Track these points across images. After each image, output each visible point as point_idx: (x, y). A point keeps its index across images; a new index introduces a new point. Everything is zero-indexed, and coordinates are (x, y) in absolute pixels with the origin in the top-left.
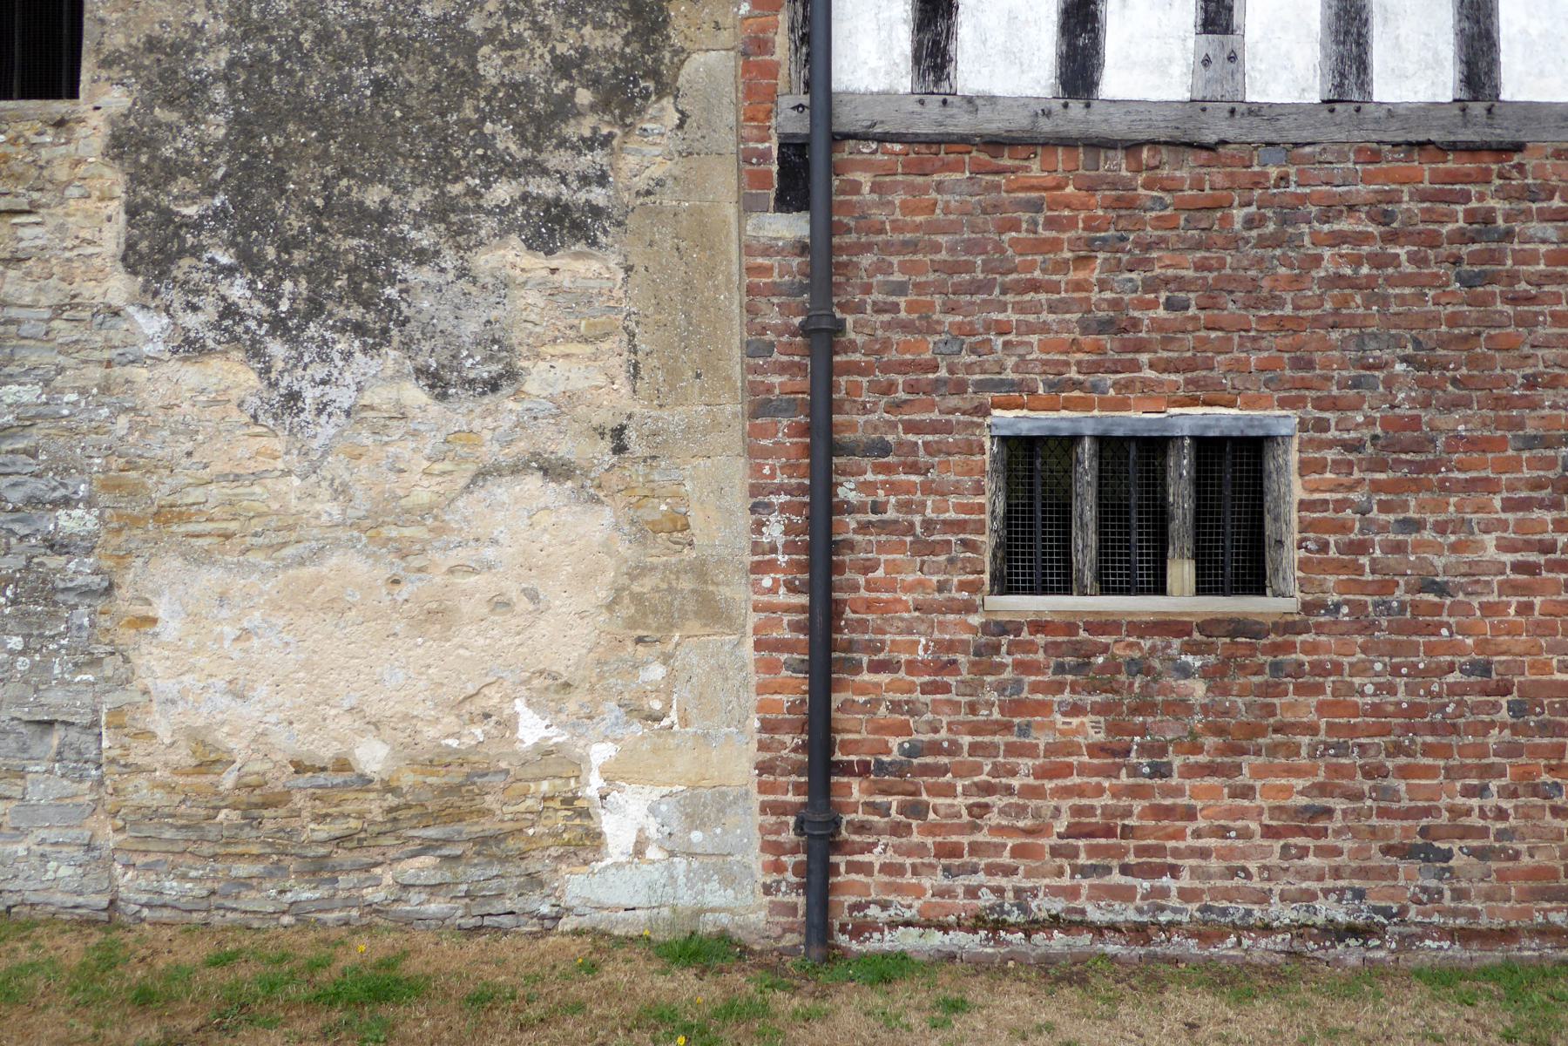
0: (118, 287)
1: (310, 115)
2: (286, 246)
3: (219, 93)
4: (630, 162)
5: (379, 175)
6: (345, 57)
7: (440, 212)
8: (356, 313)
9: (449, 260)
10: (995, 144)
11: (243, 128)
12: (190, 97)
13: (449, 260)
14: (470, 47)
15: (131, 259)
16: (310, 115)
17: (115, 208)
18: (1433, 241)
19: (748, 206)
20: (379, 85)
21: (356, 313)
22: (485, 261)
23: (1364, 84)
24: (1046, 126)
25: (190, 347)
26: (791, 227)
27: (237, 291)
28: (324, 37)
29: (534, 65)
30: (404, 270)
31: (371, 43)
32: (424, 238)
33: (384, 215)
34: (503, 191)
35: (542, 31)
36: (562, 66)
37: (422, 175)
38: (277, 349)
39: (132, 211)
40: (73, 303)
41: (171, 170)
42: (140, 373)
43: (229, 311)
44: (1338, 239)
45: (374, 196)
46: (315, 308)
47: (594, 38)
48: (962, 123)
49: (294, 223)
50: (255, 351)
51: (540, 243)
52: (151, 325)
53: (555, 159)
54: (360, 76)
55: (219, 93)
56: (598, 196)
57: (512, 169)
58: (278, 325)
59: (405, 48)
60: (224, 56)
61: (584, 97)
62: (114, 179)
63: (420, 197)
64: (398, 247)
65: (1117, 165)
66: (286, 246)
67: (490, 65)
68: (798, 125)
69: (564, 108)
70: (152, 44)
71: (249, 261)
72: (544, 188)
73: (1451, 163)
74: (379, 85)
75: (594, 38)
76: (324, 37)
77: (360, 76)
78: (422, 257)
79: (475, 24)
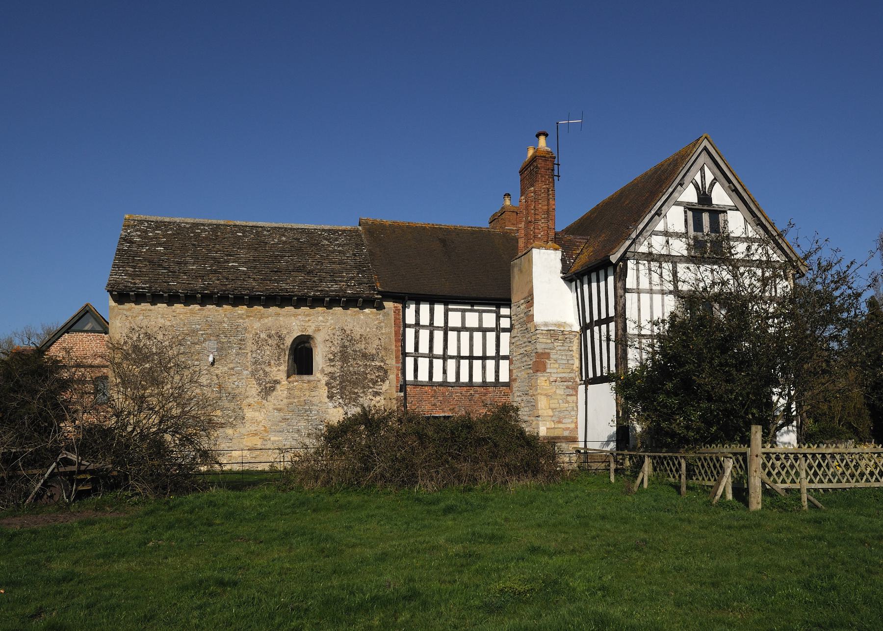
0: (327, 400)
1: (349, 381)
2: (346, 396)
3: (338, 378)
4: (384, 387)
5: (357, 388)
6: (352, 375)
7: (364, 392)
8: (354, 403)
9: (365, 398)
10: (422, 386)
12: (335, 379)
13: (365, 398)
14: (367, 374)
15: (328, 397)
16: (349, 381)
17: (326, 391)
18: (466, 396)
19: (397, 392)
20: (356, 378)
21: (354, 403)
24: (428, 384)
25: (335, 407)
26: (402, 394)
27: (341, 401)
28: (350, 373)
29: (373, 377)
30: (360, 399)
31: (355, 373)
32: (362, 395)
33: (357, 393)
34: (370, 390)
35: (375, 373)
36: (377, 377)
37: (361, 388)
39: (328, 392)
40: (321, 402)
42: (329, 410)
43: (340, 403)
44: (457, 396)
45: (356, 391)
47: (380, 374)
48: (419, 383)
49: (347, 394)
50: (343, 408)
52: (331, 404)
53: (376, 387)
54: (354, 377)
55: (338, 378)
56: (381, 391)
57: (371, 388)
58: (345, 405)
59: (359, 374)
60: (338, 374)
61: (379, 380)
62: (326, 388)
63: (361, 391)
64: (359, 396)
65: (435, 388)
66: (346, 396)
67: (369, 376)
69: (377, 381)
70: (330, 373)
71: (342, 398)
72: (375, 390)
73: (468, 388)
74: (356, 378)
75: (380, 374)
76: (350, 373)
77: (354, 377)
78: (362, 397)
79: (367, 372)
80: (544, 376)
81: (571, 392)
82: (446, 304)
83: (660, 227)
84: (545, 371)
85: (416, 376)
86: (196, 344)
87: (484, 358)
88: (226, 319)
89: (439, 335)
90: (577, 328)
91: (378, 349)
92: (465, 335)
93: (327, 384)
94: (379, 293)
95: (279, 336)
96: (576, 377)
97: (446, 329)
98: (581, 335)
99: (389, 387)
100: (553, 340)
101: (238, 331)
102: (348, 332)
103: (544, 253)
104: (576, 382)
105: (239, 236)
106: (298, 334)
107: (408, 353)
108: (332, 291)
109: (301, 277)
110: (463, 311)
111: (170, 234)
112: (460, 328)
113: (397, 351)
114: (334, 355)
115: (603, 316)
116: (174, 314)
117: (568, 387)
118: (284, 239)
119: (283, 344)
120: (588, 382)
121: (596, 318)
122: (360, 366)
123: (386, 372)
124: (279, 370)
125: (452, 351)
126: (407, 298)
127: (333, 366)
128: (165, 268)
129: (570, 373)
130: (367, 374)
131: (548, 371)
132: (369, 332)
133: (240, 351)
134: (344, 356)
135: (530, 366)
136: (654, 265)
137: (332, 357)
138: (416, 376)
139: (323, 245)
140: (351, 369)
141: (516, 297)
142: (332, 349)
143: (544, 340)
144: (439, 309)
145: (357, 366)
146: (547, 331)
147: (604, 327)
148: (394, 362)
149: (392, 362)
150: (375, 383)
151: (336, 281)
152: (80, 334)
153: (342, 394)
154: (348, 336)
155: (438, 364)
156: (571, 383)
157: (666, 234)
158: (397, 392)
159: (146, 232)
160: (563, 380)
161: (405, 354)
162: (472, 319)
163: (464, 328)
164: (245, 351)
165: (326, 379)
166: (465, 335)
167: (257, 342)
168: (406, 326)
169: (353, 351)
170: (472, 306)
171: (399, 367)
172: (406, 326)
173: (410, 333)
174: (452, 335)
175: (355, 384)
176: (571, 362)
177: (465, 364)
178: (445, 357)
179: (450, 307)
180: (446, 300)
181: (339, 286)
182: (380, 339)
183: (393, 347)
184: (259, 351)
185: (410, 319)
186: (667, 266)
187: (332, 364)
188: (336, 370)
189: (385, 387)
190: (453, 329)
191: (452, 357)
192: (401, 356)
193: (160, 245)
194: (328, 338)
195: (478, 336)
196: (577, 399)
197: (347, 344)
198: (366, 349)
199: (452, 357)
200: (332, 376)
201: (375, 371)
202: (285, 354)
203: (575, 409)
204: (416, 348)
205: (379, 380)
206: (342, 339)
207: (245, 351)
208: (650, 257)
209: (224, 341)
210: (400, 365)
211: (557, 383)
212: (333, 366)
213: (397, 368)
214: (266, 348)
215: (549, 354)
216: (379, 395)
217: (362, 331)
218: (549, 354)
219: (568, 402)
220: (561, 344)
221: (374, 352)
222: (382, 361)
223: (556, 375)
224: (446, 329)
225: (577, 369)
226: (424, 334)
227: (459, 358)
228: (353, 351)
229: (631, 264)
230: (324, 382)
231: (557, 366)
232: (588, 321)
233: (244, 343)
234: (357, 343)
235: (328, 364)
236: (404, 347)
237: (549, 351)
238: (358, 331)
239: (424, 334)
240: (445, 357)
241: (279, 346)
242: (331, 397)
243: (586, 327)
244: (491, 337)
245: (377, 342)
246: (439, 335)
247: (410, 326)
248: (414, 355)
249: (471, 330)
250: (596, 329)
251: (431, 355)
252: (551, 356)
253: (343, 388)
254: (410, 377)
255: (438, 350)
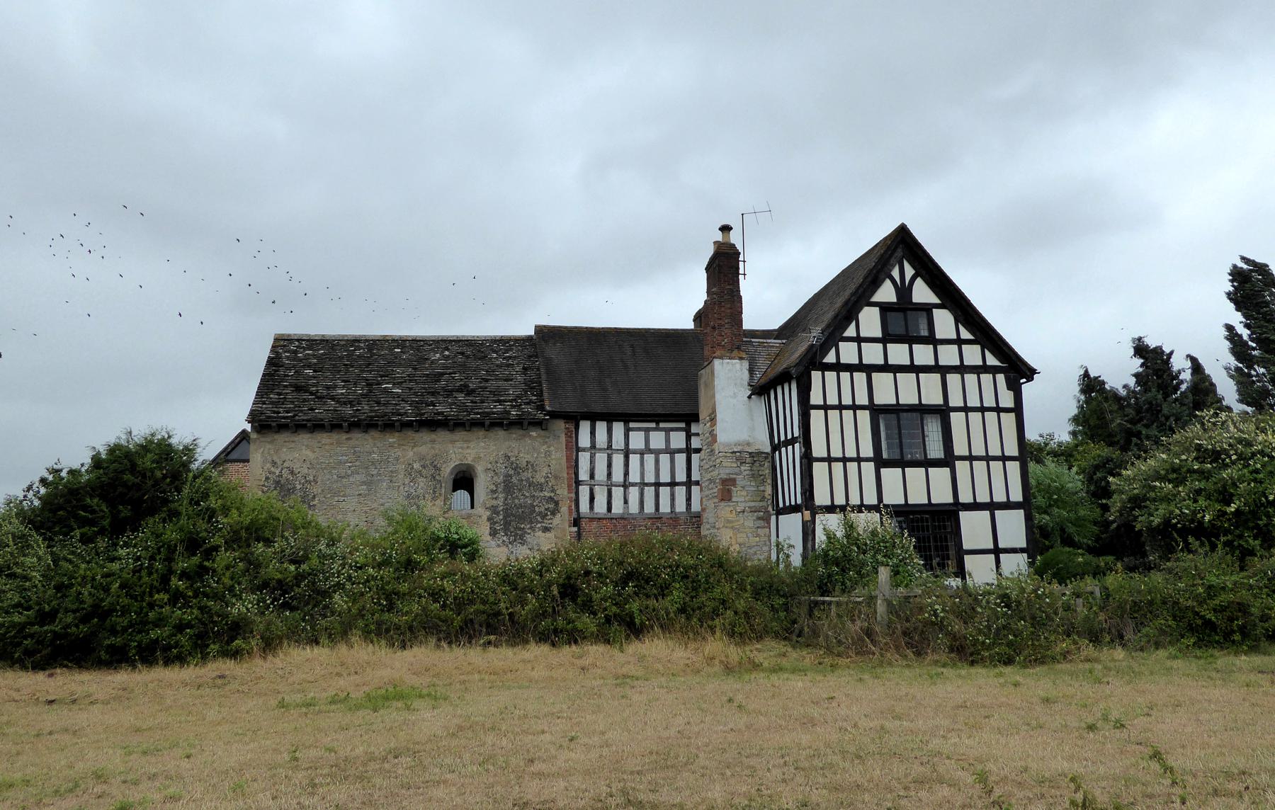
0: (489, 538)
3: (501, 513)
7: (531, 528)
10: (599, 519)
11: (505, 517)
14: (534, 507)
15: (490, 535)
17: (488, 528)
19: (570, 526)
22: (536, 534)
23: (644, 511)
24: (606, 517)
25: (499, 546)
26: (575, 529)
27: (505, 538)
29: (543, 510)
32: (529, 531)
33: (524, 528)
34: (539, 525)
35: (543, 505)
36: (546, 509)
37: (528, 524)
38: (510, 546)
41: (496, 523)
43: (504, 541)
45: (522, 526)
46: (515, 540)
47: (550, 506)
48: (595, 516)
49: (512, 530)
50: (507, 546)
51: (544, 532)
53: (545, 521)
55: (501, 513)
56: (551, 526)
57: (541, 523)
58: (510, 543)
60: (502, 508)
63: (528, 526)
64: (526, 532)
67: (537, 509)
68: (576, 516)
69: (547, 515)
70: (492, 506)
71: (506, 535)
75: (550, 506)
76: (515, 505)
78: (529, 534)
79: (535, 504)
80: (729, 506)
81: (761, 523)
82: (626, 422)
83: (851, 331)
84: (730, 500)
85: (592, 508)
86: (343, 477)
87: (673, 484)
88: (375, 449)
89: (618, 460)
90: (768, 449)
91: (548, 477)
92: (650, 459)
93: (489, 519)
94: (549, 413)
95: (435, 466)
96: (768, 506)
97: (627, 453)
98: (773, 458)
99: (561, 521)
100: (739, 463)
101: (389, 462)
102: (513, 459)
103: (728, 363)
104: (769, 511)
105: (398, 352)
106: (456, 463)
107: (581, 481)
108: (494, 413)
109: (461, 397)
110: (647, 430)
111: (322, 354)
112: (642, 450)
113: (569, 479)
114: (496, 486)
115: (789, 437)
116: (320, 445)
117: (759, 518)
118: (447, 353)
119: (439, 474)
120: (780, 512)
121: (783, 438)
122: (527, 497)
123: (557, 503)
124: (434, 505)
125: (634, 477)
126: (579, 417)
127: (496, 498)
128: (312, 394)
129: (760, 501)
130: (534, 507)
131: (734, 499)
132: (537, 457)
133: (391, 484)
134: (508, 487)
135: (716, 494)
136: (845, 376)
137: (495, 489)
138: (592, 508)
139: (491, 359)
140: (516, 501)
141: (703, 415)
142: (495, 478)
143: (729, 464)
144: (618, 428)
145: (524, 498)
146: (732, 453)
147: (790, 448)
148: (566, 492)
149: (563, 492)
150: (544, 516)
151: (499, 401)
152: (236, 464)
153: (506, 530)
154: (512, 463)
155: (618, 493)
156: (762, 513)
157: (859, 340)
158: (570, 526)
159: (295, 352)
160: (753, 510)
161: (578, 483)
162: (657, 440)
163: (648, 450)
164: (396, 484)
165: (488, 513)
166: (650, 459)
167: (410, 474)
168: (578, 450)
169: (519, 480)
170: (657, 423)
171: (572, 497)
172: (578, 450)
173: (584, 459)
174: (635, 460)
175: (521, 518)
176: (762, 488)
177: (650, 491)
178: (626, 485)
179: (632, 425)
180: (626, 418)
181: (502, 407)
182: (549, 466)
183: (565, 475)
184: (412, 484)
185: (584, 441)
186: (860, 377)
187: (495, 496)
188: (500, 502)
189: (557, 520)
190: (635, 452)
191: (634, 485)
192: (574, 485)
193: (309, 367)
194: (489, 466)
195: (664, 458)
196: (770, 532)
197: (511, 472)
198: (533, 478)
199: (634, 485)
200: (494, 509)
201: (544, 503)
202: (441, 486)
203: (768, 544)
204: (592, 476)
205: (549, 513)
206: (506, 468)
207: (396, 484)
208: (838, 367)
209: (374, 473)
210: (573, 495)
211: (745, 513)
212: (496, 498)
213: (570, 499)
214: (420, 480)
215: (734, 480)
216: (548, 530)
217: (528, 458)
218: (734, 480)
219: (758, 536)
220: (749, 468)
221: (543, 480)
222: (552, 491)
223: (743, 504)
224: (627, 453)
225: (769, 497)
226: (601, 459)
227: (643, 485)
228: (519, 480)
229: (816, 376)
230: (485, 518)
231: (744, 493)
232: (776, 441)
233: (395, 475)
234: (523, 471)
235: (490, 496)
236: (577, 474)
237: (734, 476)
238: (525, 458)
239: (601, 459)
240: (626, 485)
241: (434, 477)
242: (493, 533)
243: (776, 448)
244: (681, 459)
245: (546, 470)
246: (618, 460)
247: (584, 450)
248: (589, 483)
249: (657, 453)
250: (783, 450)
251: (609, 482)
252: (737, 482)
253: (506, 525)
254: (584, 507)
255: (618, 476)
